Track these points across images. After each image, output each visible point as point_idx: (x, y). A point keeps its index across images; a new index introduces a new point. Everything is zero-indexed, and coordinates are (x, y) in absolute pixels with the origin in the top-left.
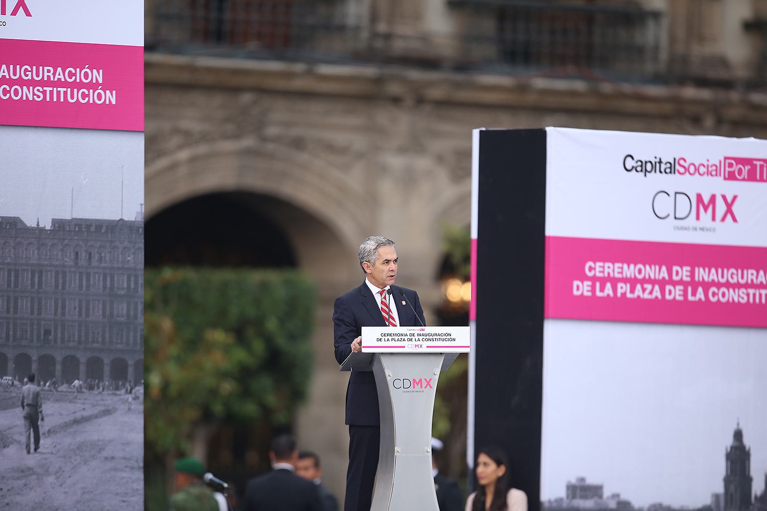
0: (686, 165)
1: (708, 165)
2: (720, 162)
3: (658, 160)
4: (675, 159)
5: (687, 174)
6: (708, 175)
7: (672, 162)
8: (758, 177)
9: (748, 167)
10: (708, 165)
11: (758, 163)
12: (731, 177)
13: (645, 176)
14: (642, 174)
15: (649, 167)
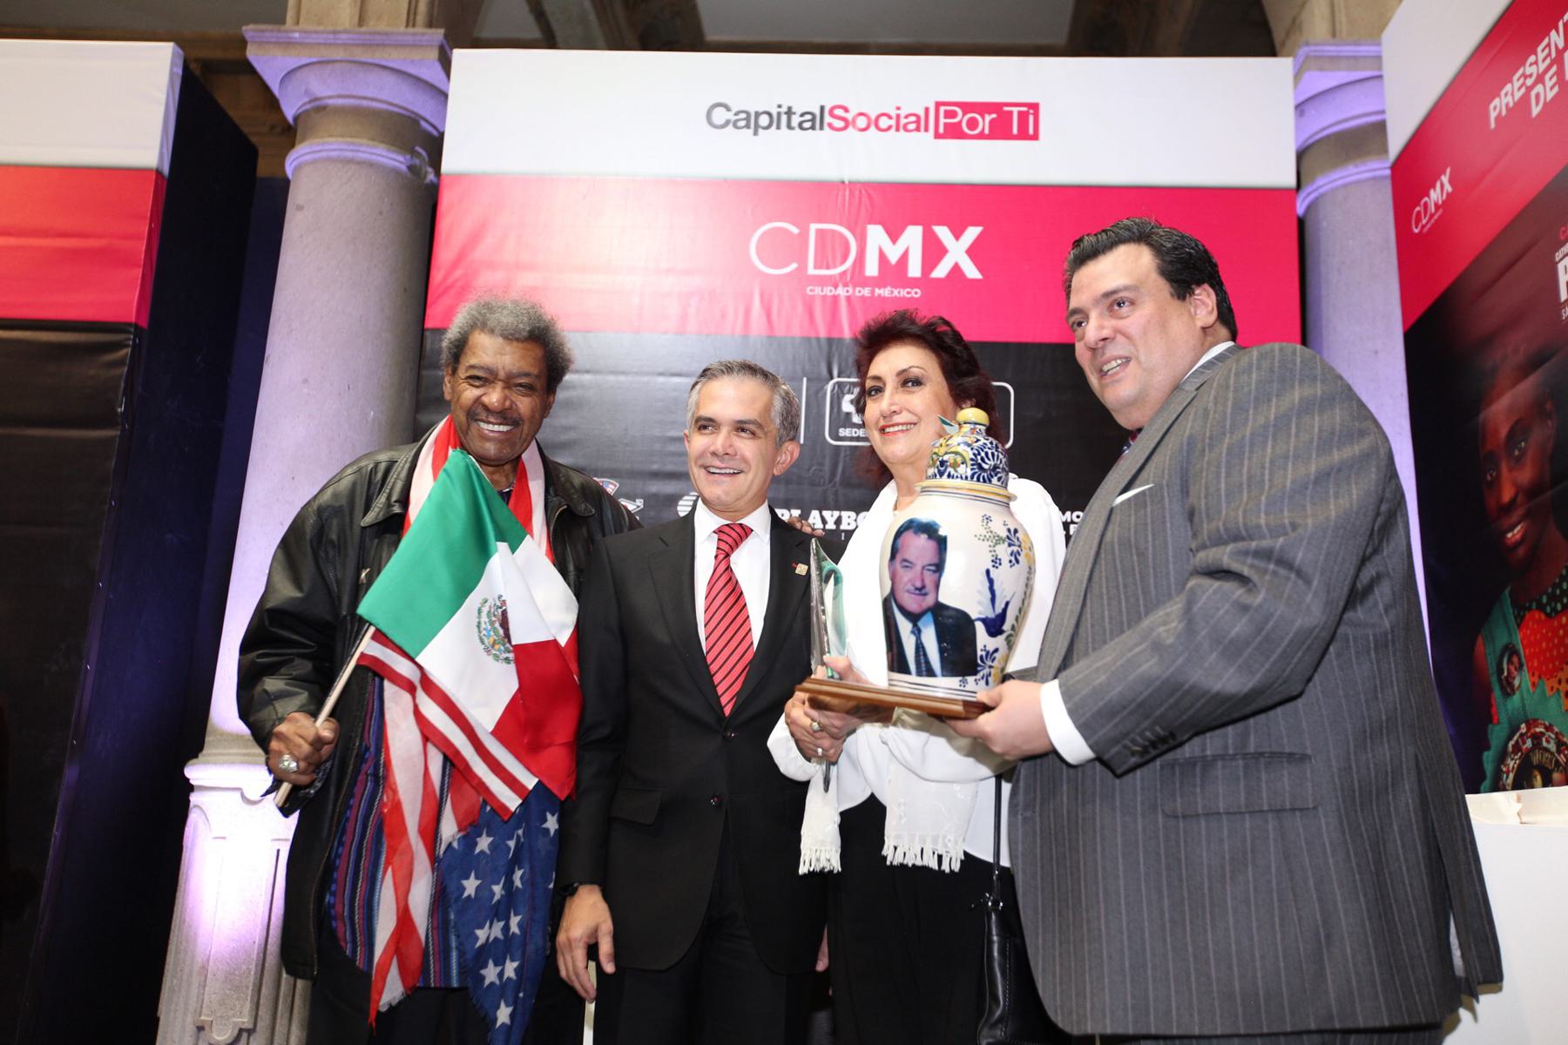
0: (849, 116)
1: (898, 116)
2: (927, 110)
3: (784, 109)
4: (822, 108)
5: (851, 129)
6: (898, 129)
7: (817, 112)
8: (1015, 131)
9: (988, 118)
10: (898, 116)
11: (1015, 110)
12: (954, 132)
13: (756, 133)
14: (751, 131)
15: (764, 120)
